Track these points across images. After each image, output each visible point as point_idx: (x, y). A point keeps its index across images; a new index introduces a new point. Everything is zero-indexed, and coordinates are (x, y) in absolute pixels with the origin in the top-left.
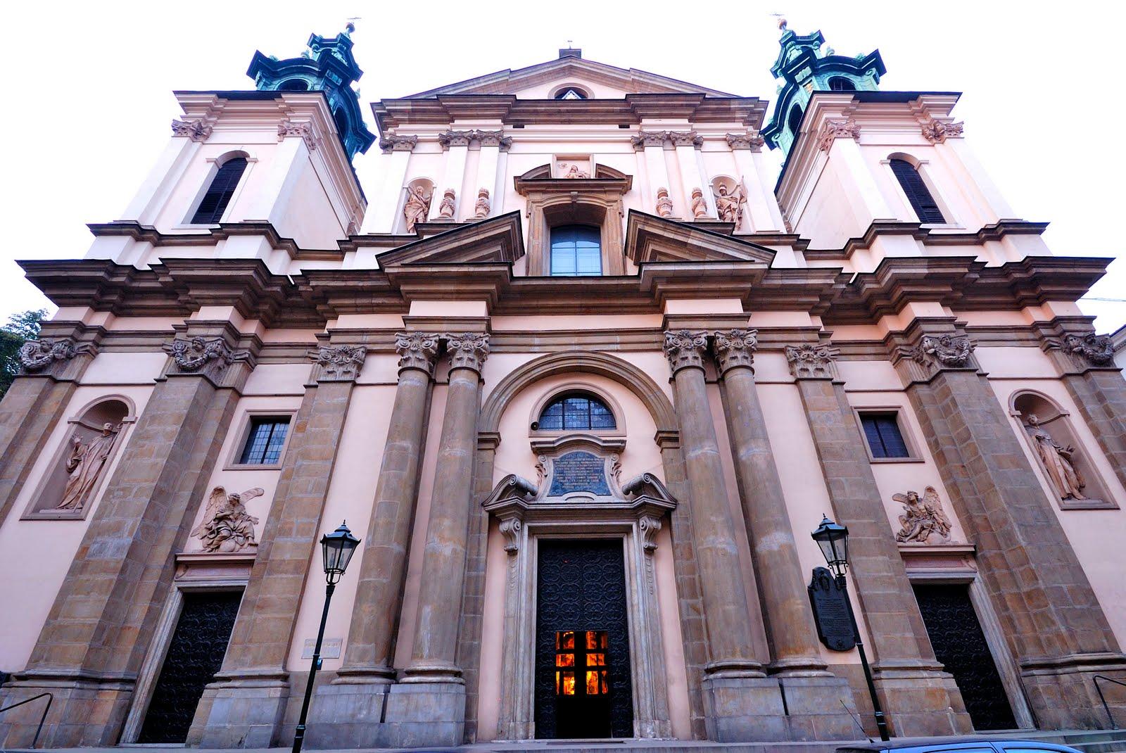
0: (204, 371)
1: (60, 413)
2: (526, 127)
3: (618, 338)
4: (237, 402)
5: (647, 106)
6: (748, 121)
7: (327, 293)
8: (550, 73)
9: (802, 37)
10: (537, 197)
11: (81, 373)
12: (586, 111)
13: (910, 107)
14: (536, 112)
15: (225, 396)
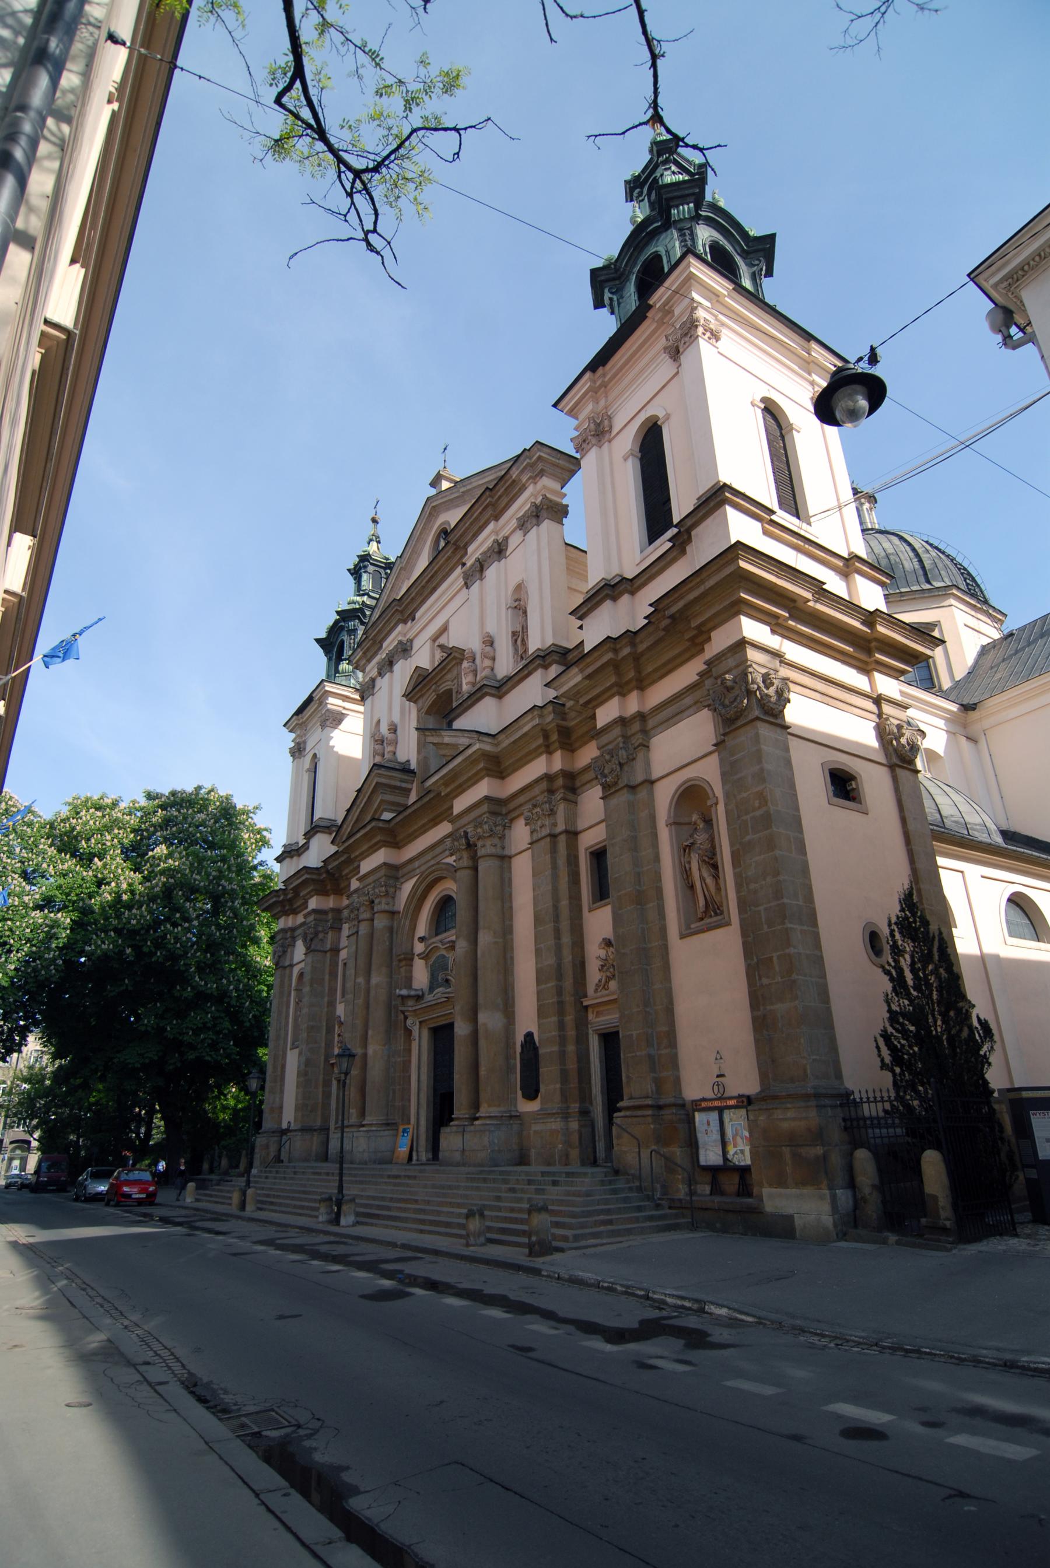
0: (313, 947)
1: (290, 985)
2: (418, 615)
4: (338, 955)
5: (461, 536)
6: (536, 476)
7: (339, 868)
8: (424, 528)
9: (643, 171)
10: (420, 702)
11: (292, 959)
12: (436, 572)
15: (328, 955)
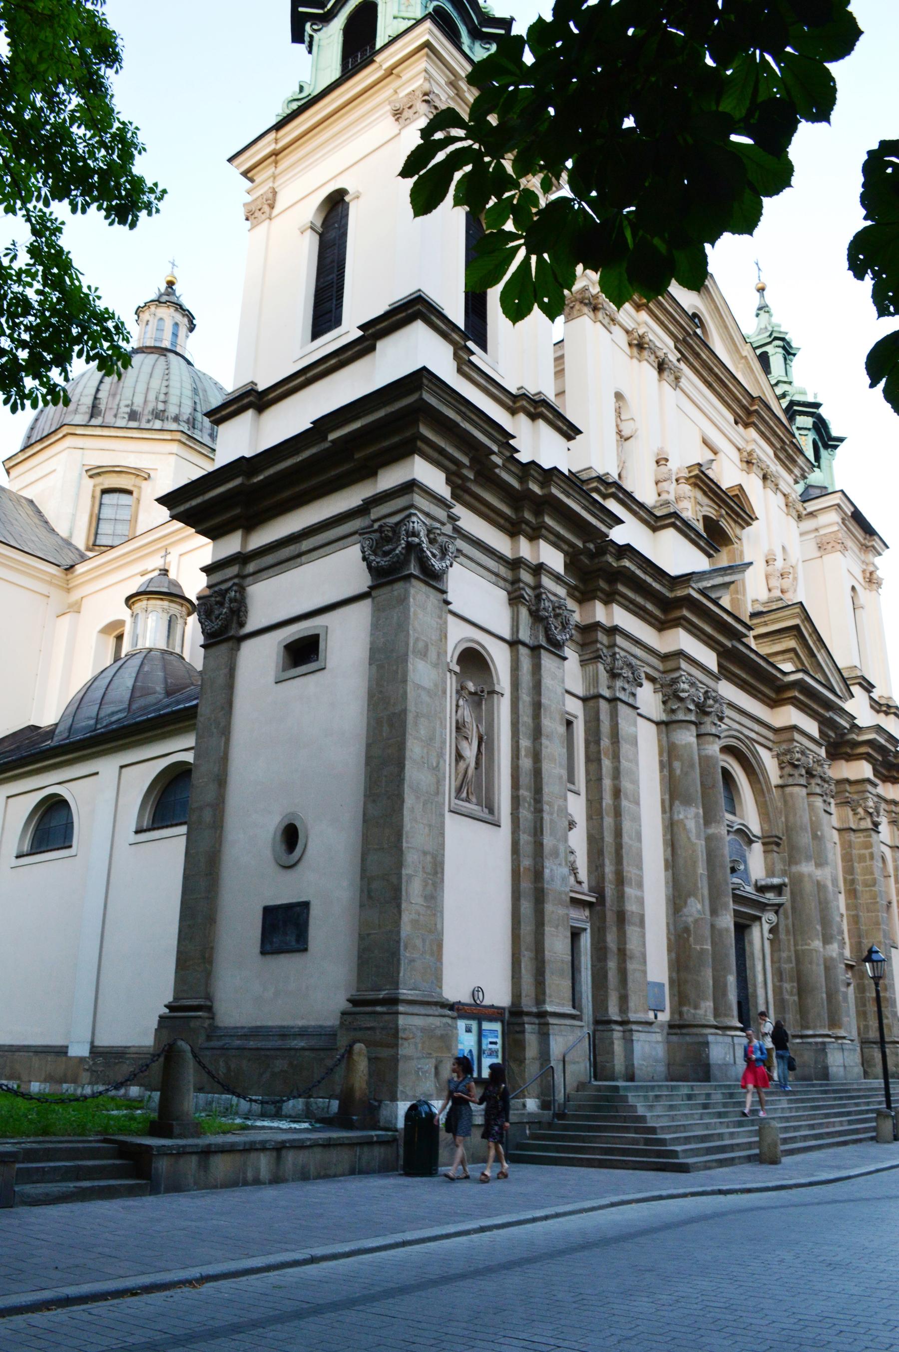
3: (756, 727)
13: (865, 539)
14: (697, 356)
